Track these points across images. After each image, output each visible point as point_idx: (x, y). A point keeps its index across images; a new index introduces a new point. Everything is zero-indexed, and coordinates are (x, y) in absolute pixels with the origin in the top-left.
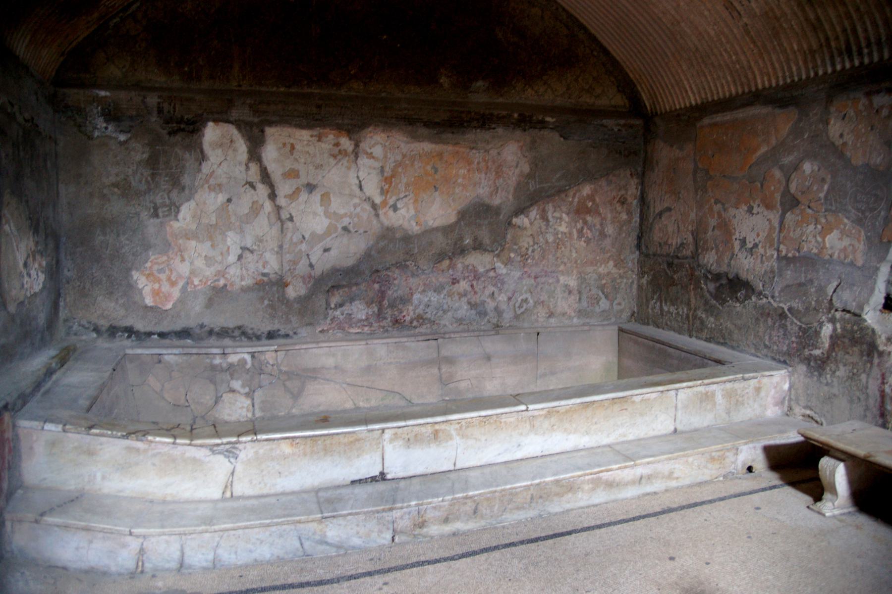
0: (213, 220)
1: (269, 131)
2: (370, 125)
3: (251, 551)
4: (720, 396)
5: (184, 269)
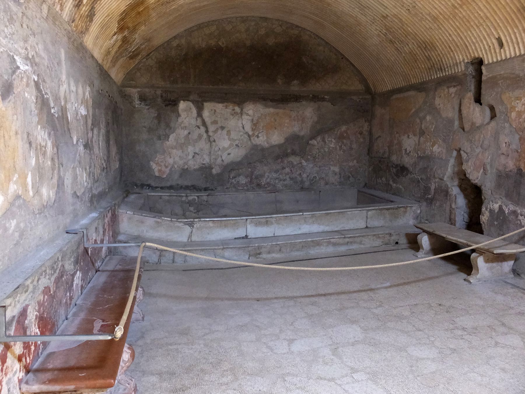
0: (183, 141)
1: (206, 104)
2: (247, 102)
5: (171, 161)
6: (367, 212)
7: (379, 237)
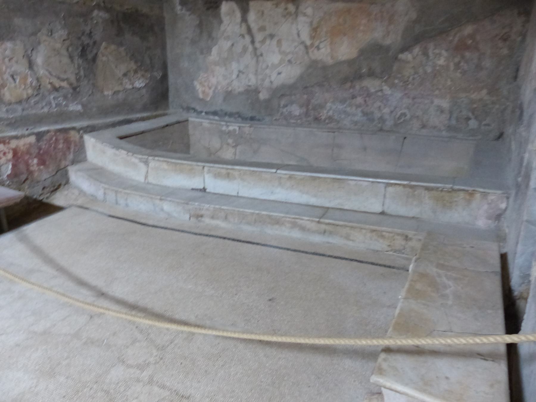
5: (214, 81)
7: (383, 237)
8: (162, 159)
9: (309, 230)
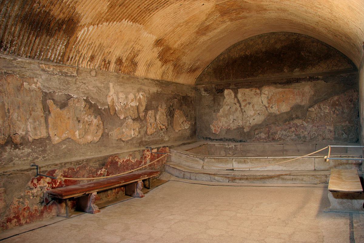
1: (239, 90)
3: (202, 178)
4: (331, 161)
5: (221, 124)
6: (315, 159)
7: (317, 177)
8: (212, 157)
9: (285, 179)
